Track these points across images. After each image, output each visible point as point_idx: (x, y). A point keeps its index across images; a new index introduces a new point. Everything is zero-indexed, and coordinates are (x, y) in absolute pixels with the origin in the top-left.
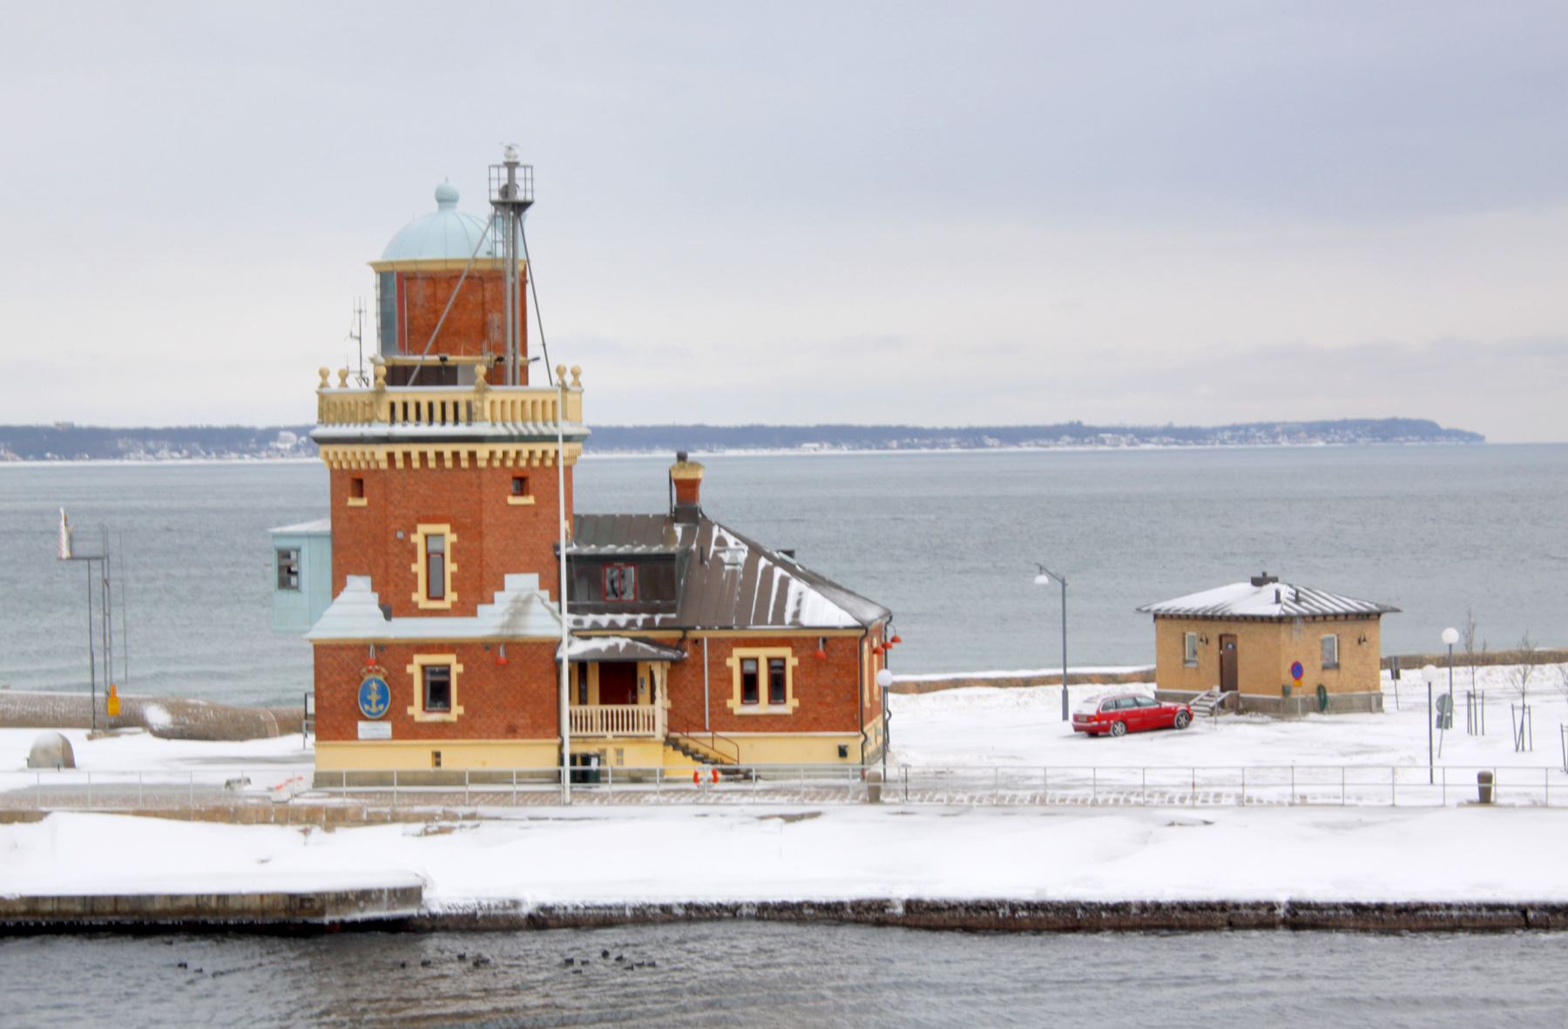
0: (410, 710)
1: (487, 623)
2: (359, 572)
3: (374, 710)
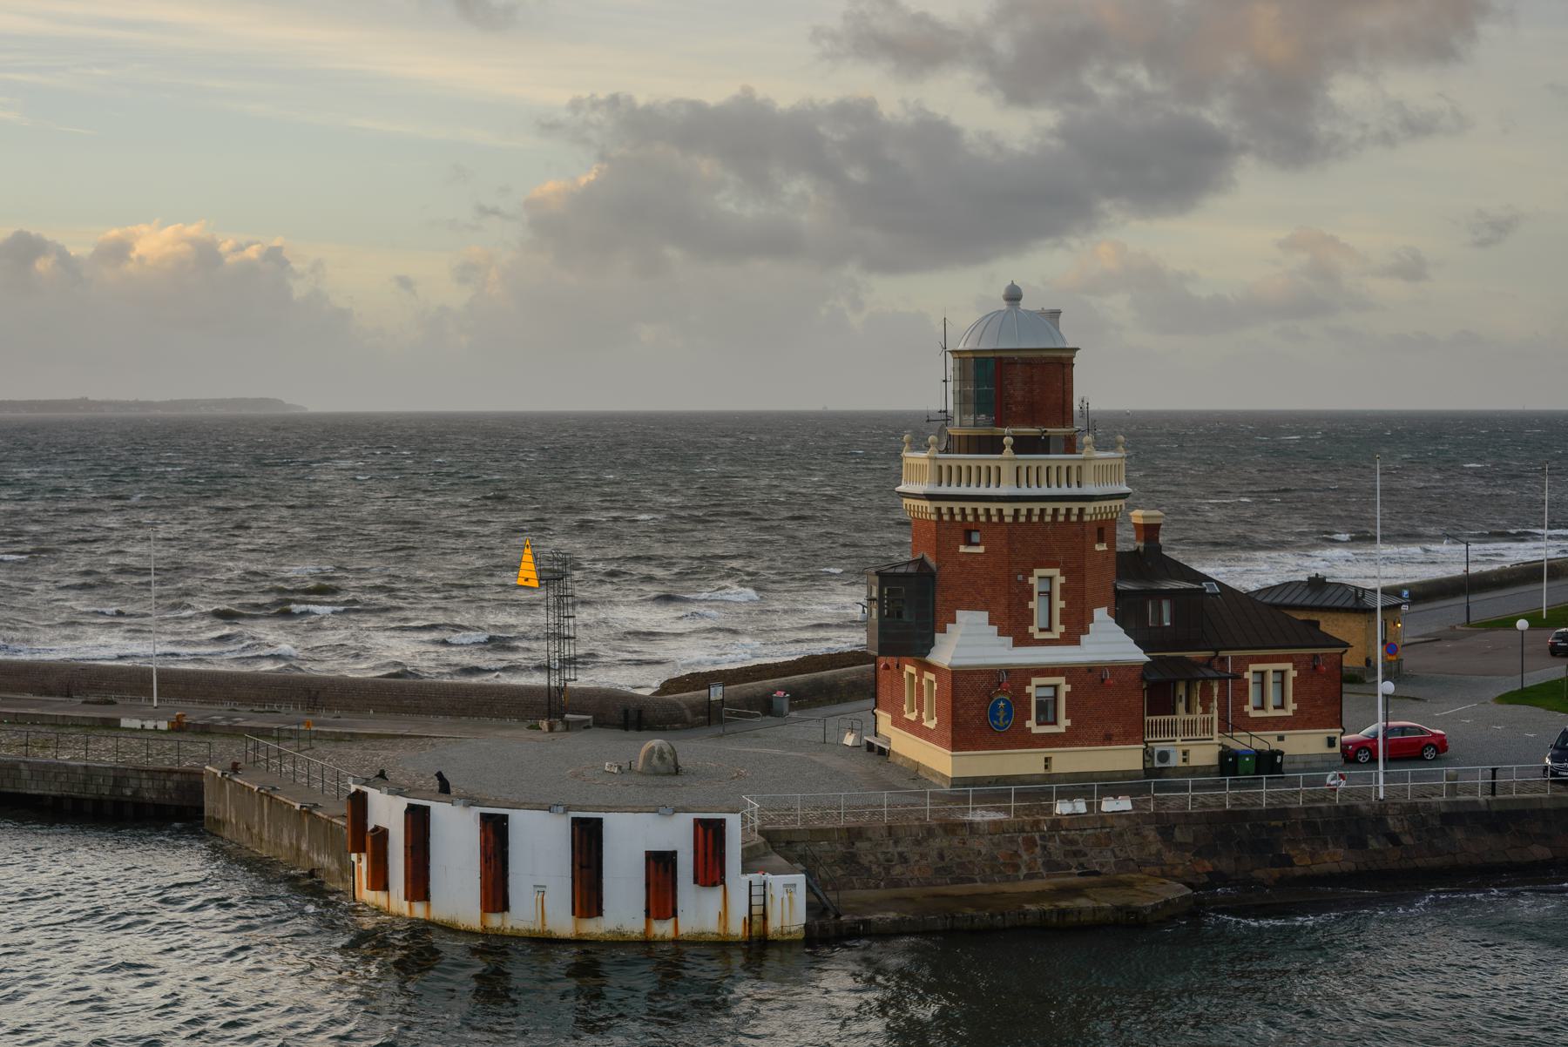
3: (1001, 724)
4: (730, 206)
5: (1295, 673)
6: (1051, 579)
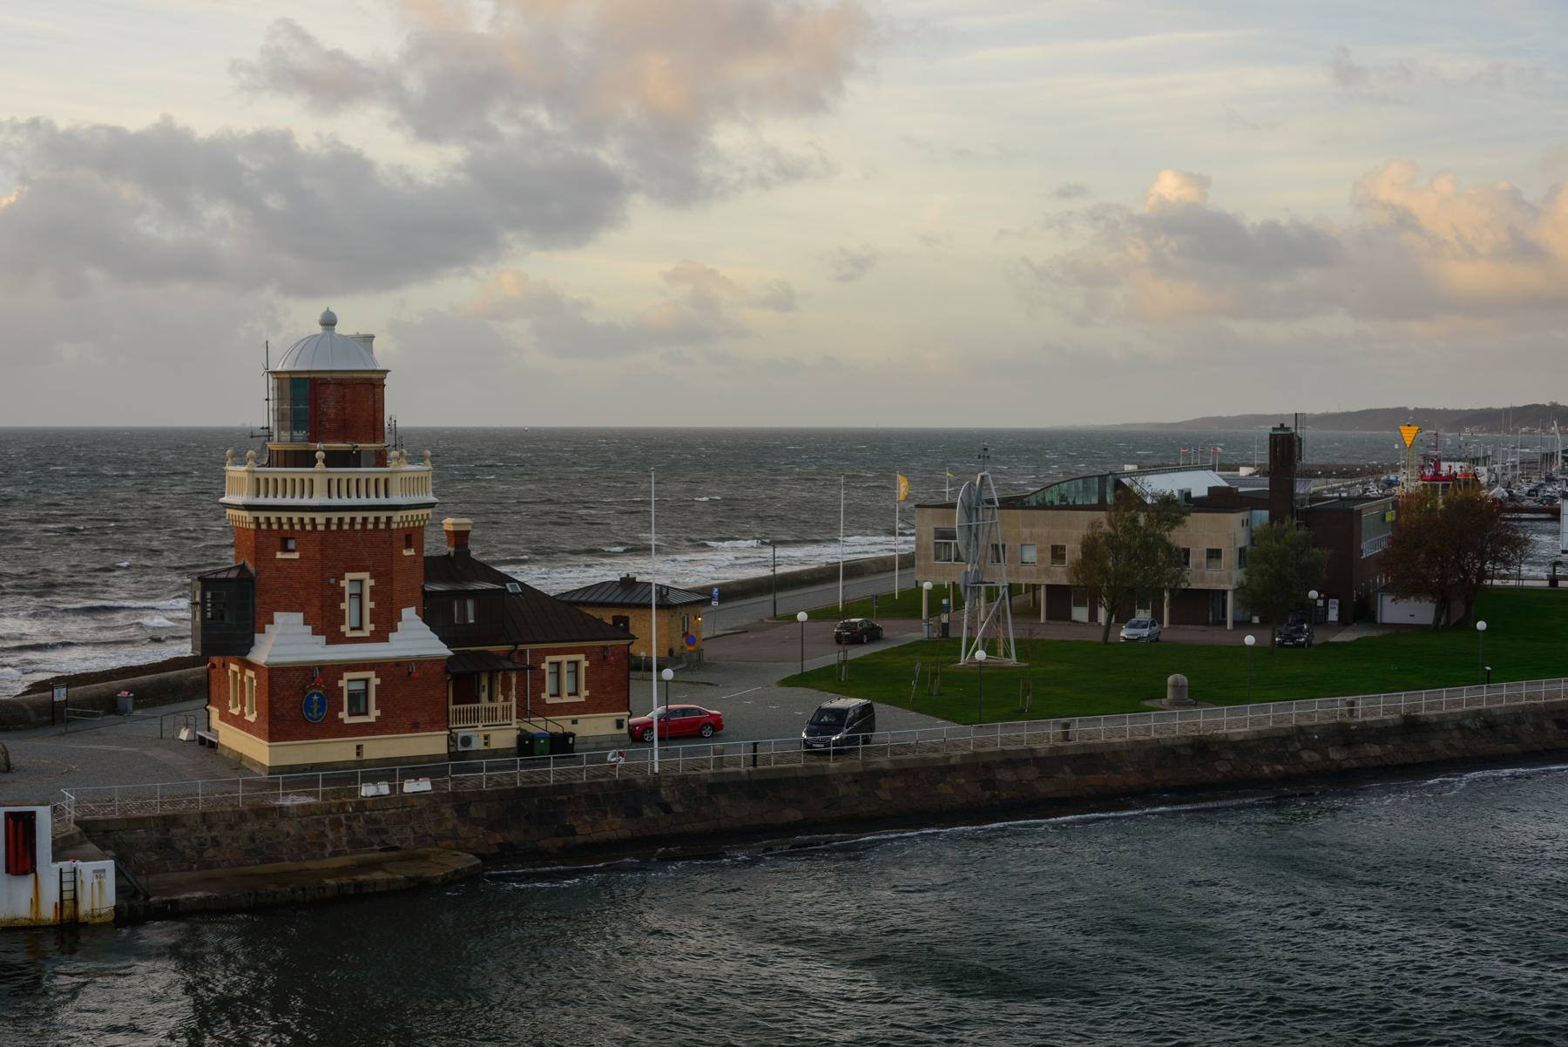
0: (341, 715)
2: (288, 608)
4: (151, 230)
5: (586, 664)
6: (361, 581)
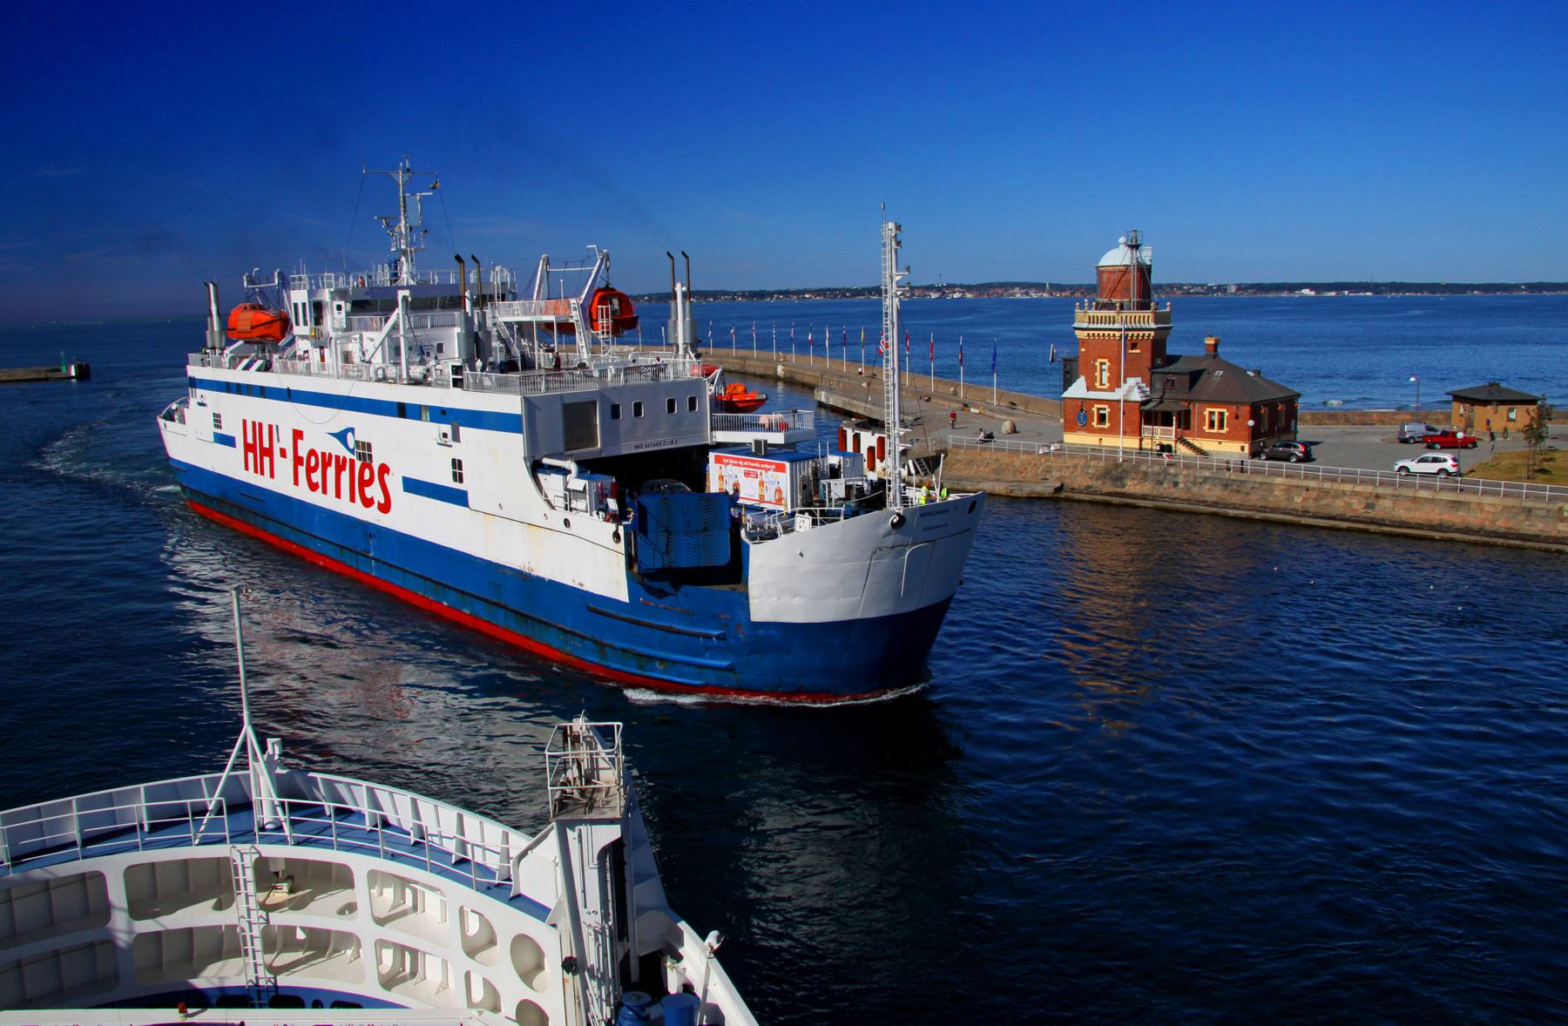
1: (1118, 395)
